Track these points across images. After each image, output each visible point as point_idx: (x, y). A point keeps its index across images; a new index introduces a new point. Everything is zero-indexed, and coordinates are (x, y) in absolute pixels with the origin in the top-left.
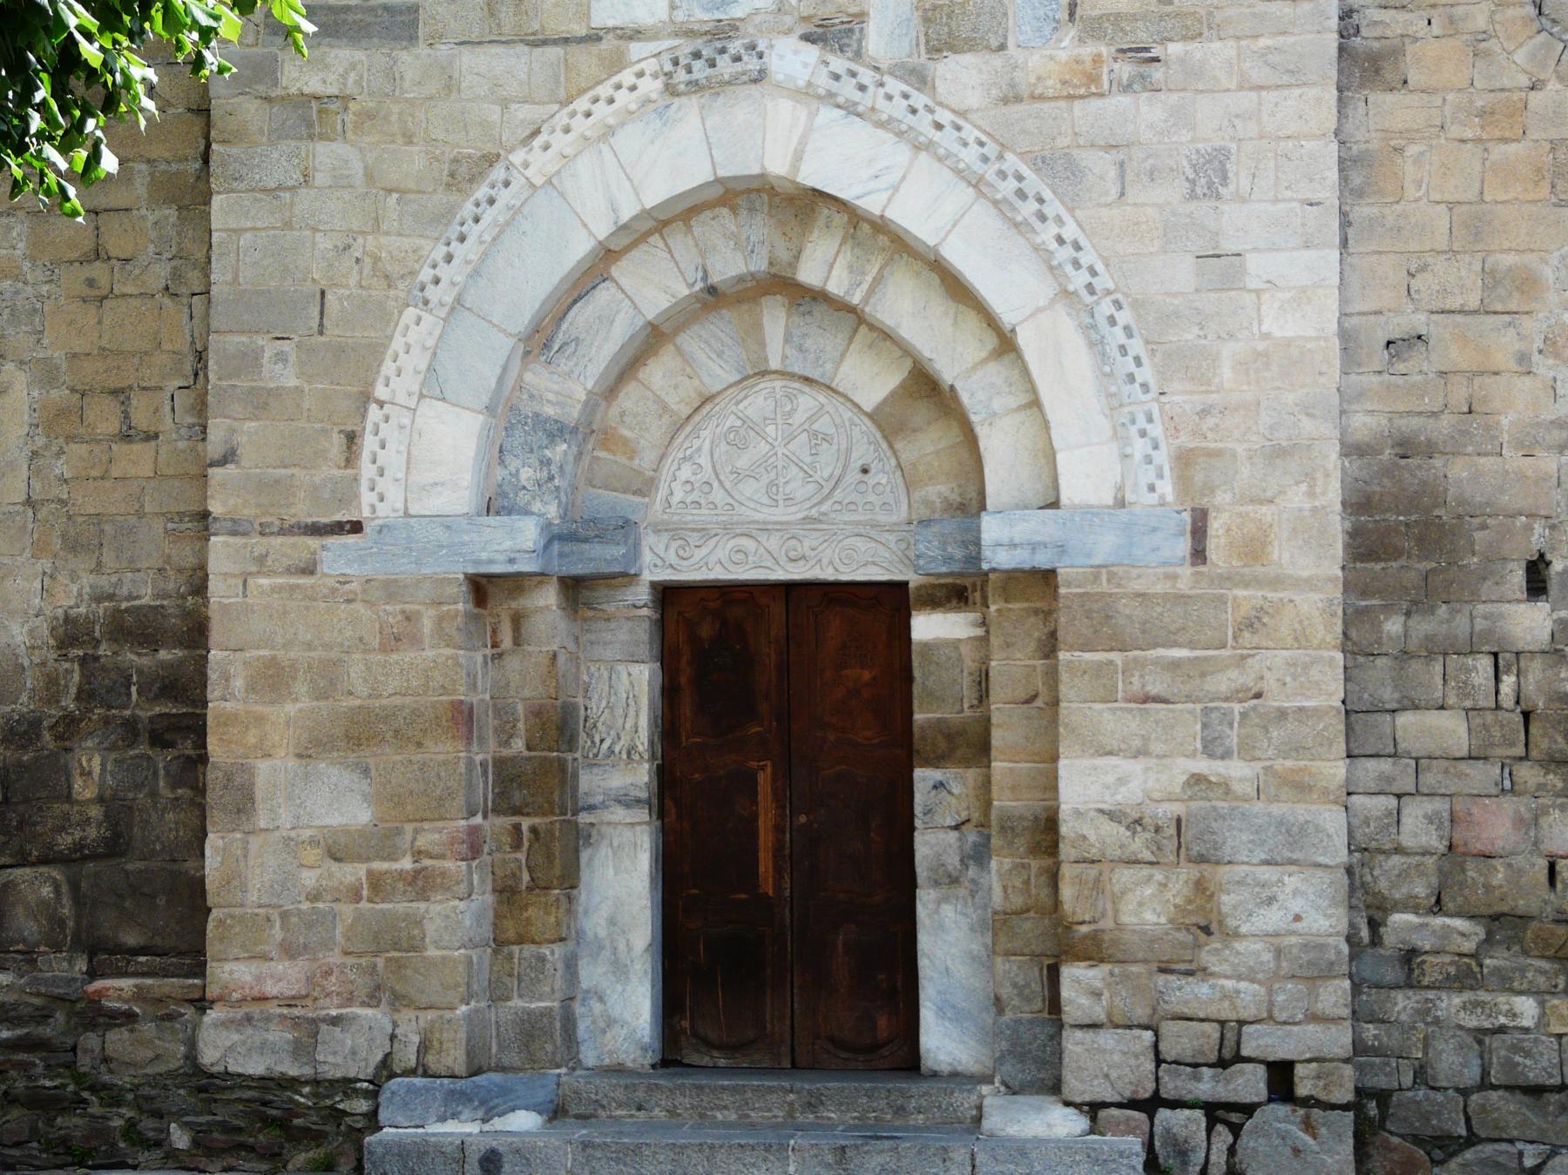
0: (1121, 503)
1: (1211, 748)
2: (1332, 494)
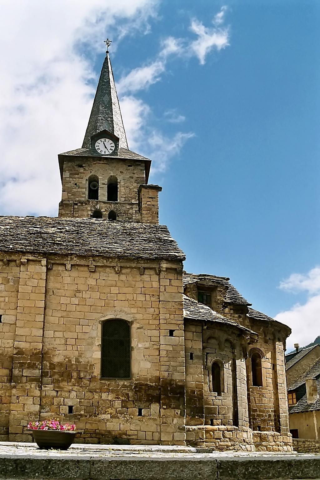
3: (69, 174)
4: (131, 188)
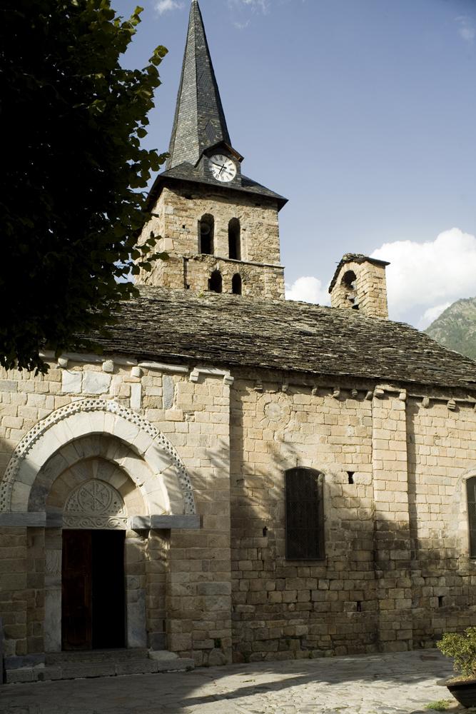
0: (184, 513)
1: (203, 570)
2: (228, 513)
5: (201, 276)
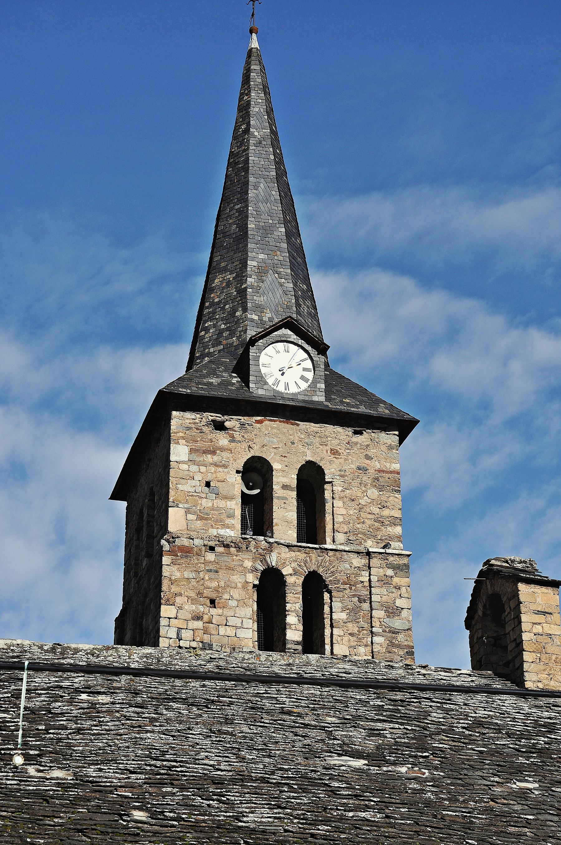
3: (186, 450)
4: (363, 502)
5: (237, 579)
